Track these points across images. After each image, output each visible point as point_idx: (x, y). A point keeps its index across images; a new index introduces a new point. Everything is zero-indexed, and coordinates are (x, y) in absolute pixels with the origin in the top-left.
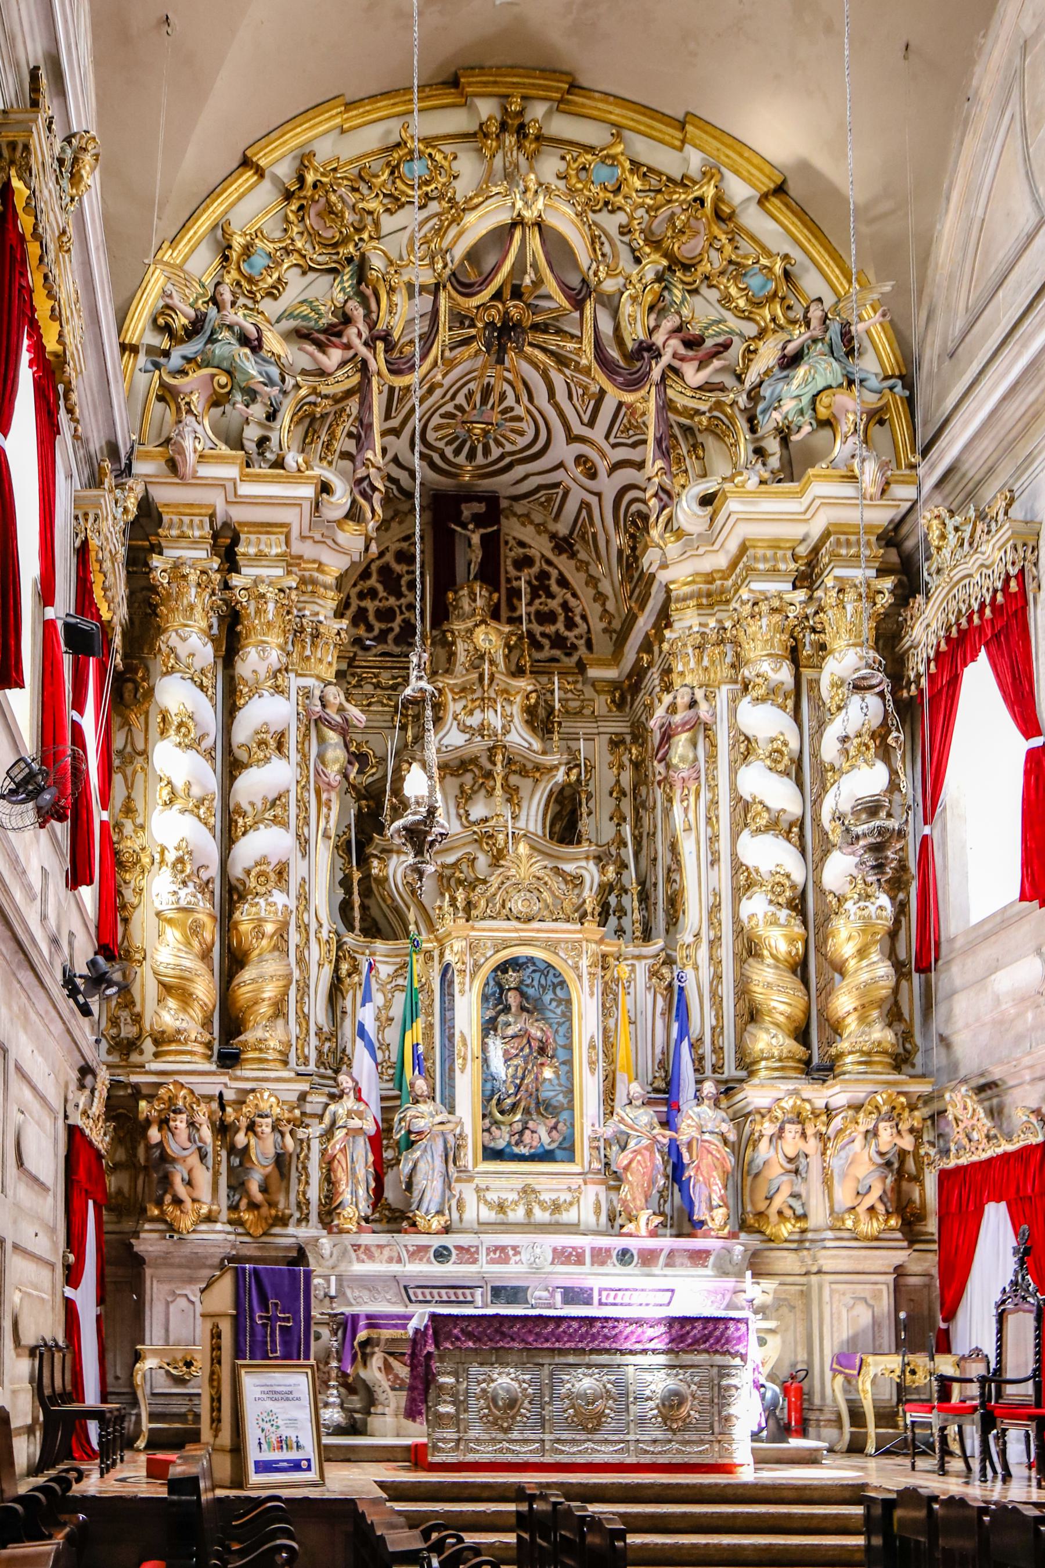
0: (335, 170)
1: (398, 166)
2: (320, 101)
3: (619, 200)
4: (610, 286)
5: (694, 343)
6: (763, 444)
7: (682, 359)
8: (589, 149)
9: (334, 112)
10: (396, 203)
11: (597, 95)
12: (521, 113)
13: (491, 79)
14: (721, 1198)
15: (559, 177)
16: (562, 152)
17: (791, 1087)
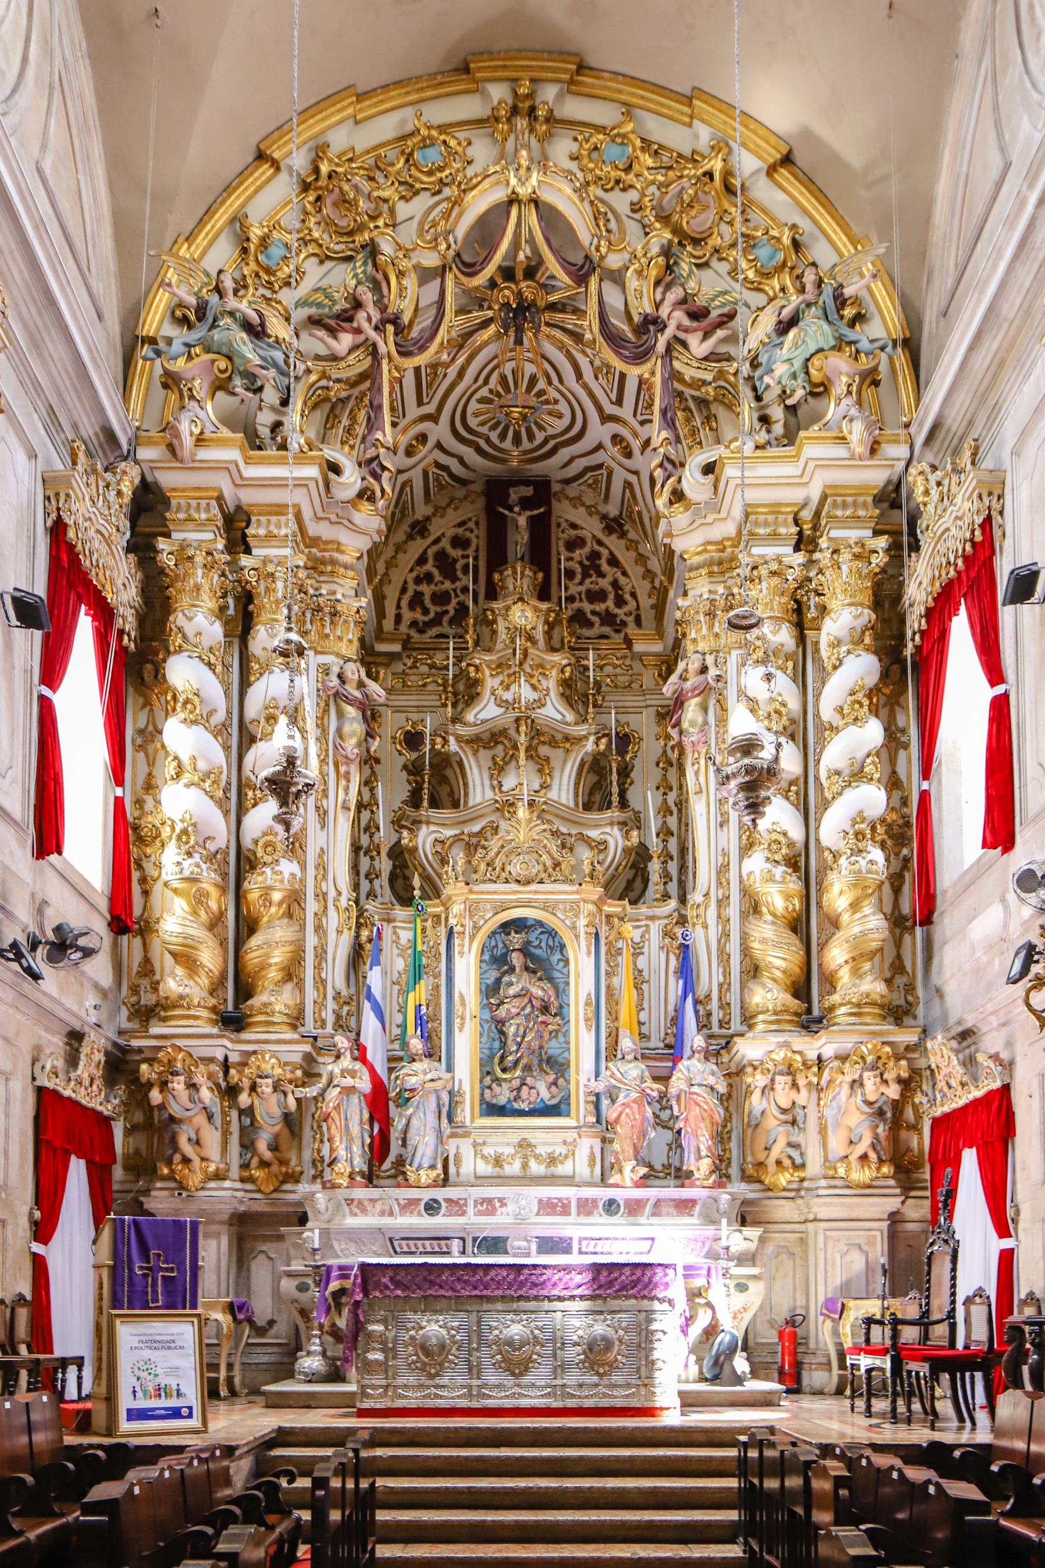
0: (351, 160)
1: (411, 154)
2: (330, 92)
3: (630, 178)
5: (698, 315)
6: (768, 411)
8: (600, 129)
9: (346, 103)
10: (411, 191)
11: (606, 75)
12: (530, 96)
13: (500, 63)
14: (709, 1148)
15: (574, 158)
16: (574, 133)
17: (782, 1040)
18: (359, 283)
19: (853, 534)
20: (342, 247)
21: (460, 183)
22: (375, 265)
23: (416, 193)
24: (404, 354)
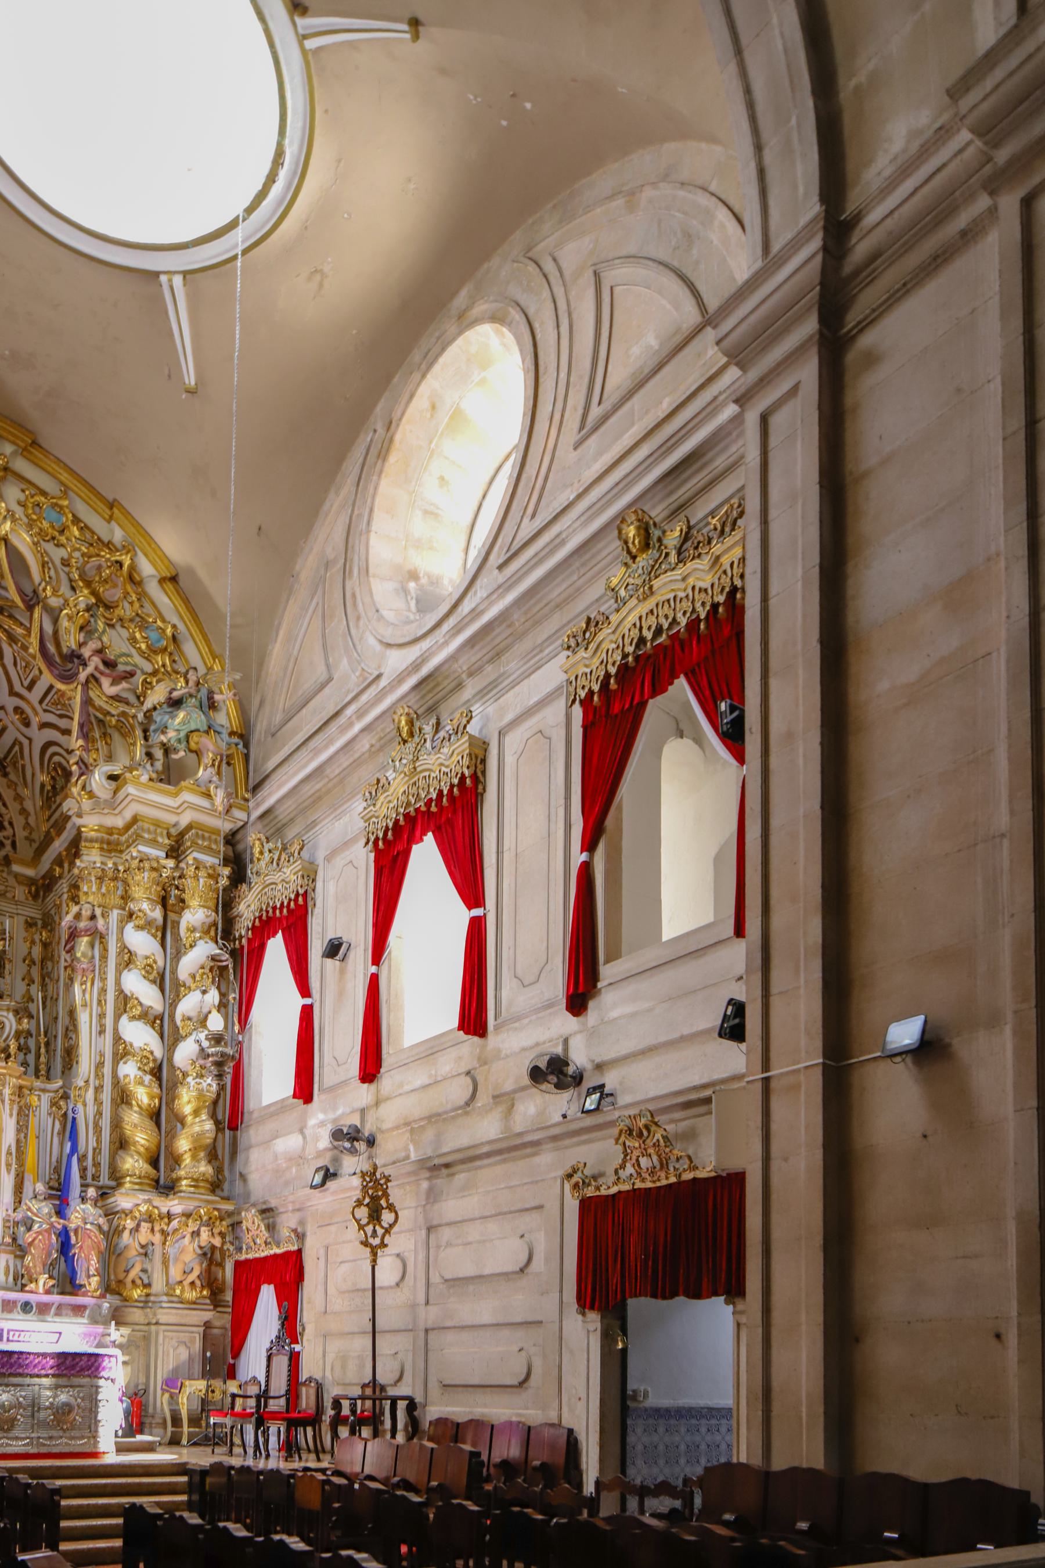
3: (63, 539)
5: (110, 664)
8: (44, 493)
17: (146, 1198)
19: (209, 860)
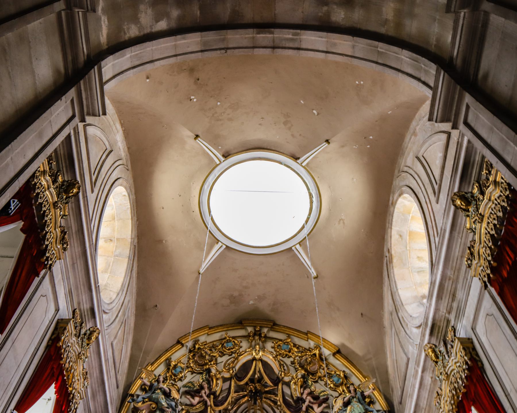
0: (205, 345)
1: (223, 344)
2: (202, 326)
3: (290, 354)
4: (287, 379)
7: (313, 403)
8: (281, 340)
9: (206, 330)
10: (222, 354)
12: (260, 330)
16: (272, 341)
18: (203, 381)
20: (200, 369)
21: (238, 353)
22: (209, 376)
23: (224, 355)
24: (216, 405)
